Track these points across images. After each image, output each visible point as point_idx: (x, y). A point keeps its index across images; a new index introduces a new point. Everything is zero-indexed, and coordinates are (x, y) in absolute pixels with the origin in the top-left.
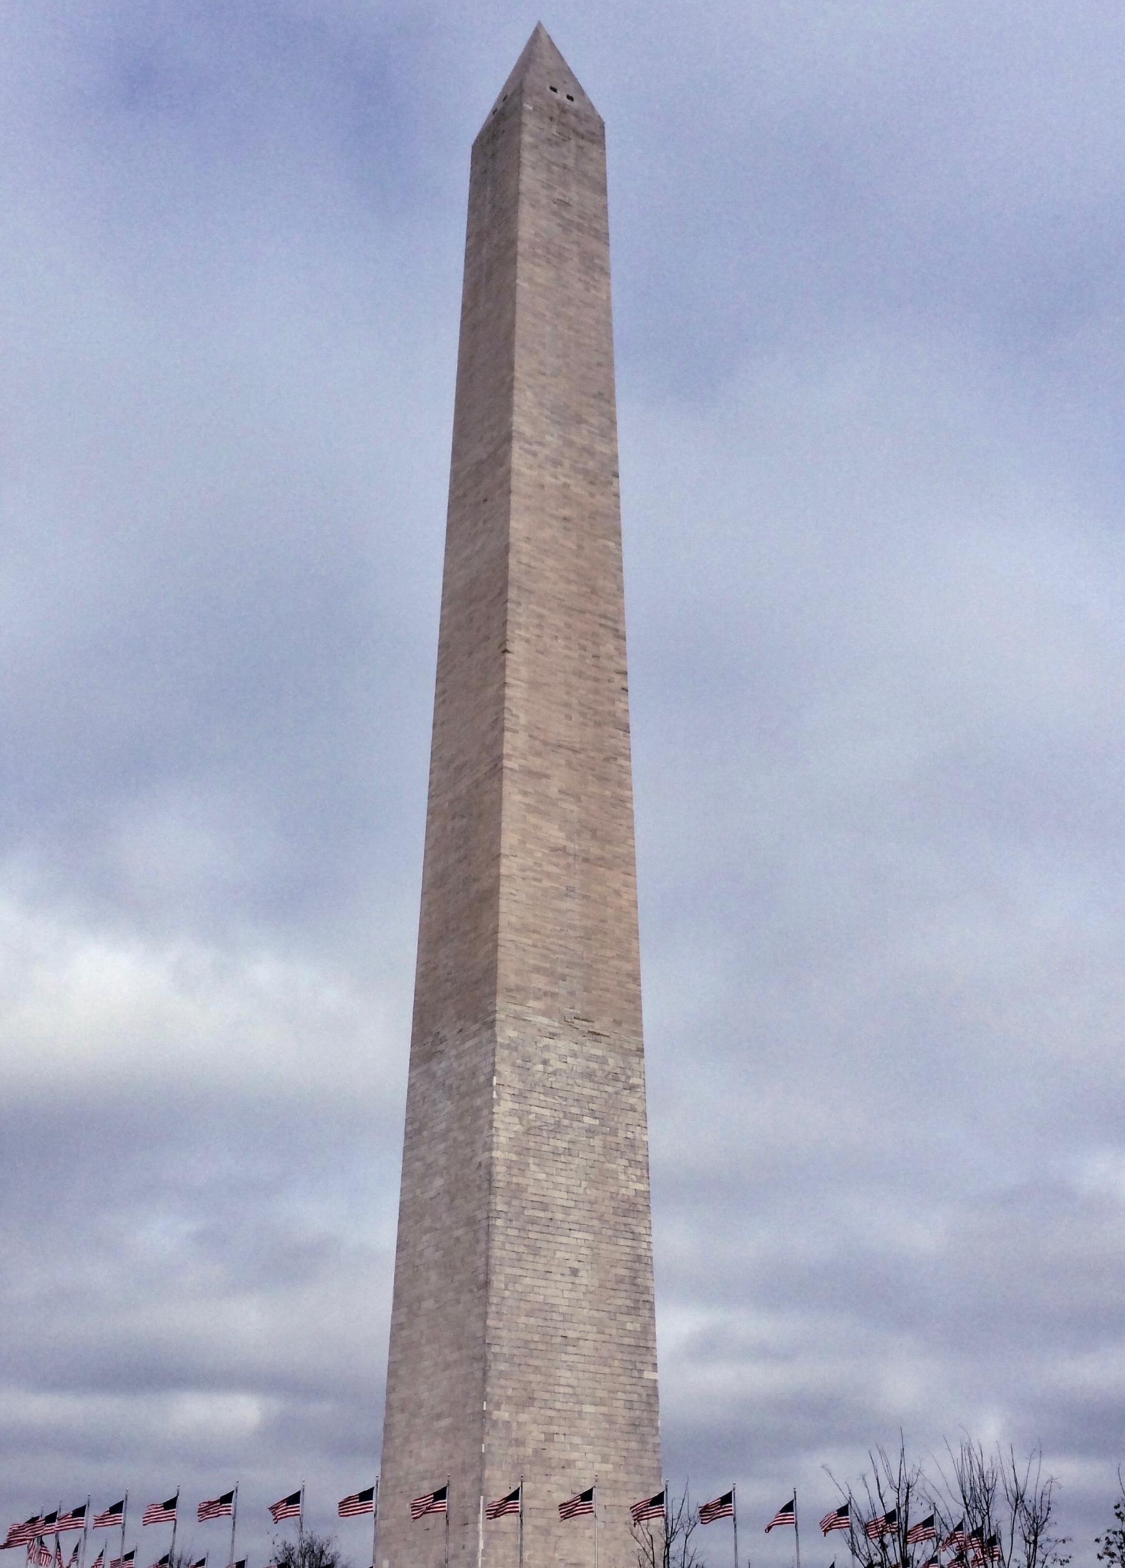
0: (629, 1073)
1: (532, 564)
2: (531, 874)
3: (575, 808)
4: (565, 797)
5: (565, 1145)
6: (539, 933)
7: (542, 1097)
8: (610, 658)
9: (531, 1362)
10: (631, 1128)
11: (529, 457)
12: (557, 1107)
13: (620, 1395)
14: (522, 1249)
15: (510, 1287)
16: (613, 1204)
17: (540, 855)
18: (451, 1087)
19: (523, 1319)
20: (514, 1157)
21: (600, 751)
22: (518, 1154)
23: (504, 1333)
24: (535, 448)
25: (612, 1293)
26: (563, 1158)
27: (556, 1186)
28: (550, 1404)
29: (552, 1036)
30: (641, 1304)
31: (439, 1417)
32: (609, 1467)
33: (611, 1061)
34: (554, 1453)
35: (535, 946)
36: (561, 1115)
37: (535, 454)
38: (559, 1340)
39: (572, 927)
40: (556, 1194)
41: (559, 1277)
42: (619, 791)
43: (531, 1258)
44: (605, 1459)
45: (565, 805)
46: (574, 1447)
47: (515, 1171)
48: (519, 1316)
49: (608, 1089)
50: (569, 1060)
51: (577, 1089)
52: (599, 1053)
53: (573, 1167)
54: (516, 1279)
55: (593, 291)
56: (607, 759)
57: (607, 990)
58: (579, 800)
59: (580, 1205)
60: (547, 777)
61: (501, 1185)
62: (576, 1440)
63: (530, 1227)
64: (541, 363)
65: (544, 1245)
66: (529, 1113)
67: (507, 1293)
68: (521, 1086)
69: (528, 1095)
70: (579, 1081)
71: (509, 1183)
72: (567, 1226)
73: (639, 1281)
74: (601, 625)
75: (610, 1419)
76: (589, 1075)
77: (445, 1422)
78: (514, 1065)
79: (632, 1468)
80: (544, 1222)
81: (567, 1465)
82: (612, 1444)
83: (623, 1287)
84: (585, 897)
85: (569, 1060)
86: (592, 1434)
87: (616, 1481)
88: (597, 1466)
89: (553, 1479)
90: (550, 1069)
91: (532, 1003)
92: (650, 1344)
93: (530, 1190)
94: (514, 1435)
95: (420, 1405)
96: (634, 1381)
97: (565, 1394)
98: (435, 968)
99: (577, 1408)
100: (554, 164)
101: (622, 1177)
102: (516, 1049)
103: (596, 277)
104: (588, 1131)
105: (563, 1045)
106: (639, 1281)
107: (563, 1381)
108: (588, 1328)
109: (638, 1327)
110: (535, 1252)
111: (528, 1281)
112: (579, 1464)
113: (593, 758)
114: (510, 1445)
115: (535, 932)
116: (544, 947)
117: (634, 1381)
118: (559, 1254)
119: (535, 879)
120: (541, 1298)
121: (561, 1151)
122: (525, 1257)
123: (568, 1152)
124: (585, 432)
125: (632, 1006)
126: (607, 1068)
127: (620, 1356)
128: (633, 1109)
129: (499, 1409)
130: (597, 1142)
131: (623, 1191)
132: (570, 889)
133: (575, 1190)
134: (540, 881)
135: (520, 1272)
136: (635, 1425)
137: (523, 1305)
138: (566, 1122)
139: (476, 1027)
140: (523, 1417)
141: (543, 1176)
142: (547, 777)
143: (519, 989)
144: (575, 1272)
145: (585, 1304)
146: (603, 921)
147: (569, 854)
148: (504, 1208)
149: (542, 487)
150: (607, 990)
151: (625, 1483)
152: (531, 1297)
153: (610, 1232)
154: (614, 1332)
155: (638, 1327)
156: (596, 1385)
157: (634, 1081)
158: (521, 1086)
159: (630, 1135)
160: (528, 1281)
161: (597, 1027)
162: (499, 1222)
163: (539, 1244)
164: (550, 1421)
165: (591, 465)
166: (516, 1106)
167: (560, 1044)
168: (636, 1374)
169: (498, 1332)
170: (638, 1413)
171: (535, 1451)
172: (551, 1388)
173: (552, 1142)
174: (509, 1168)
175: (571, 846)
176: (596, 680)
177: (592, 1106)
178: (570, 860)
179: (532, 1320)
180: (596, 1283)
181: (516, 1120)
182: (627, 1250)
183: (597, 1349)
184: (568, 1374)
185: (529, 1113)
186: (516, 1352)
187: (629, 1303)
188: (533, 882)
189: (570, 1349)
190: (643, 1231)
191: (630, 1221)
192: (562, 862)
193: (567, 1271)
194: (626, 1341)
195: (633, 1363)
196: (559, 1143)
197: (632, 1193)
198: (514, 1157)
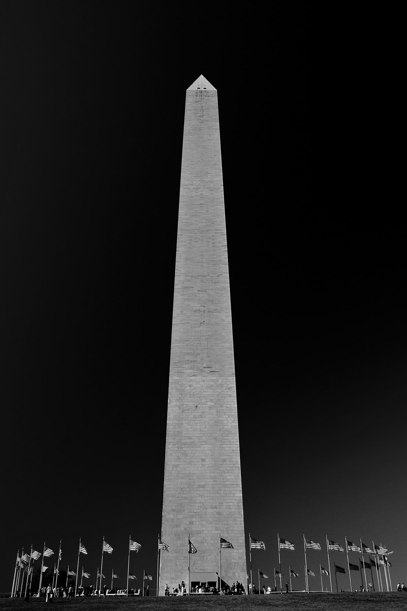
0: (228, 383)
7: (189, 398)
8: (220, 242)
9: (184, 496)
10: (229, 403)
14: (180, 454)
16: (221, 432)
17: (189, 314)
20: (177, 422)
22: (178, 420)
24: (189, 186)
25: (221, 466)
26: (198, 419)
33: (220, 380)
34: (194, 528)
43: (183, 457)
44: (217, 529)
49: (218, 390)
51: (204, 393)
52: (215, 378)
61: (171, 432)
62: (204, 523)
63: (183, 446)
67: (173, 472)
76: (210, 387)
86: (211, 520)
88: (213, 532)
90: (192, 388)
91: (184, 366)
99: (204, 511)
101: (226, 422)
105: (198, 378)
107: (197, 501)
111: (182, 466)
114: (174, 527)
118: (196, 454)
120: (188, 472)
129: (169, 514)
130: (214, 411)
134: (189, 323)
135: (177, 463)
137: (180, 475)
140: (180, 516)
143: (179, 362)
144: (203, 460)
152: (184, 472)
153: (220, 443)
154: (222, 480)
155: (233, 477)
159: (228, 406)
161: (213, 369)
162: (169, 446)
164: (192, 517)
165: (212, 185)
167: (198, 378)
170: (233, 510)
173: (193, 414)
175: (202, 309)
176: (215, 251)
177: (211, 398)
181: (178, 408)
183: (213, 488)
184: (200, 498)
185: (183, 405)
189: (201, 489)
193: (200, 460)
196: (196, 414)
198: (177, 422)
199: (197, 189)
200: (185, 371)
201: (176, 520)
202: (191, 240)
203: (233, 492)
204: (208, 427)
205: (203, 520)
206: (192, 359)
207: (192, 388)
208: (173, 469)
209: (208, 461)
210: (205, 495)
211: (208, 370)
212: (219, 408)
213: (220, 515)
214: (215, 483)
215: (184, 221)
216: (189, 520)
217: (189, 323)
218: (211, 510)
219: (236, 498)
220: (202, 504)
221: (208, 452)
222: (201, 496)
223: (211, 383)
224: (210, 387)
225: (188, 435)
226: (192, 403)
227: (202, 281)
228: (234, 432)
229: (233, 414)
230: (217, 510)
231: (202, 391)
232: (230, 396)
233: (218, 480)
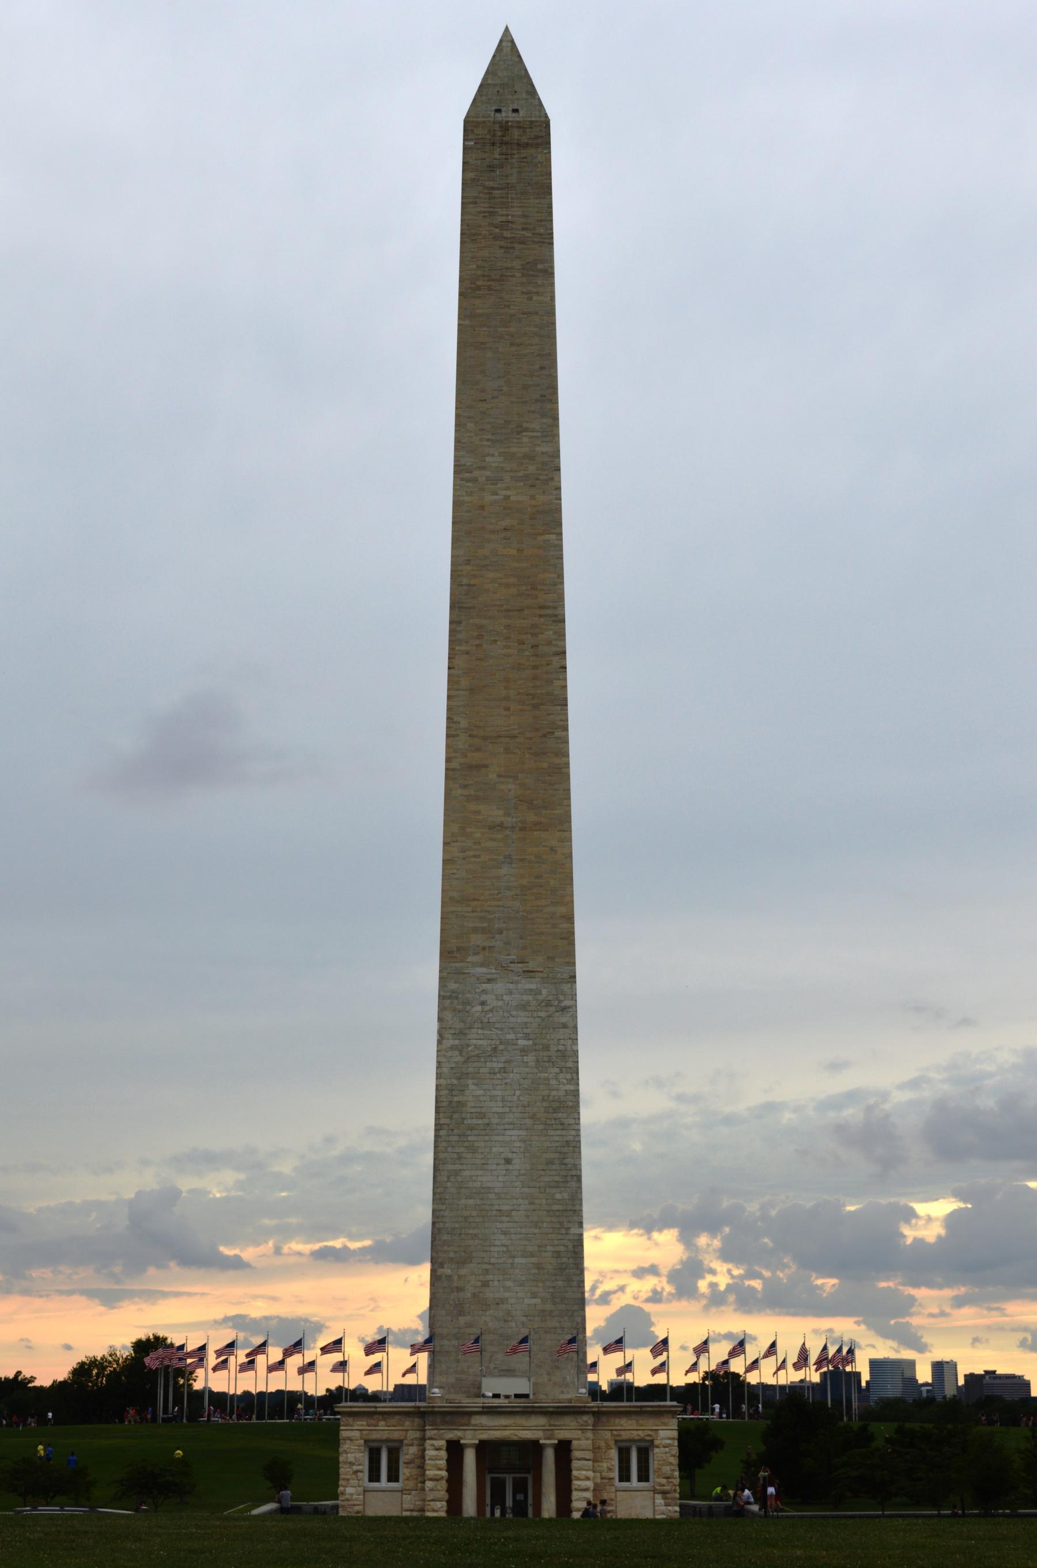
0: (562, 997)
1: (473, 582)
2: (471, 853)
3: (511, 786)
5: (501, 1065)
7: (480, 1031)
8: (549, 643)
9: (471, 1231)
11: (470, 484)
12: (494, 1037)
13: (549, 1248)
14: (462, 1150)
15: (452, 1179)
16: (545, 1104)
17: (478, 835)
20: (455, 1082)
21: (537, 730)
22: (459, 1079)
23: (446, 1214)
25: (542, 1173)
26: (498, 1076)
27: (493, 1098)
28: (486, 1260)
29: (489, 981)
32: (538, 1301)
33: (544, 992)
34: (490, 1294)
35: (473, 911)
36: (498, 1042)
37: (475, 480)
39: (509, 888)
40: (493, 1104)
41: (494, 1167)
42: (557, 761)
43: (469, 1155)
44: (534, 1295)
45: (503, 787)
46: (507, 1289)
47: (455, 1093)
48: (459, 1199)
50: (505, 997)
51: (512, 1019)
52: (533, 986)
54: (457, 1173)
55: (535, 298)
56: (545, 736)
57: (542, 933)
58: (516, 778)
60: (486, 766)
61: (444, 1104)
62: (509, 1284)
63: (469, 1132)
64: (483, 391)
65: (483, 1144)
68: (462, 1025)
69: (467, 1031)
70: (514, 1013)
71: (450, 1102)
73: (567, 1161)
74: (540, 616)
76: (523, 1007)
78: (455, 1010)
79: (557, 1300)
80: (482, 1127)
82: (540, 1284)
83: (554, 1167)
84: (522, 860)
85: (505, 997)
86: (523, 1278)
87: (543, 1311)
88: (526, 1301)
90: (487, 1008)
91: (470, 959)
92: (577, 1208)
93: (469, 1104)
94: (455, 1285)
96: (560, 1237)
97: (498, 1252)
99: (510, 1261)
100: (493, 189)
101: (553, 1082)
102: (457, 998)
103: (539, 282)
105: (500, 987)
106: (567, 1161)
107: (497, 1243)
108: (521, 1201)
109: (566, 1196)
110: (473, 1150)
111: (467, 1173)
113: (531, 739)
114: (452, 1291)
115: (474, 899)
117: (560, 1237)
118: (494, 1150)
119: (475, 856)
120: (478, 1184)
121: (497, 1070)
122: (464, 1155)
124: (525, 440)
125: (566, 942)
126: (540, 997)
127: (549, 1219)
128: (565, 1026)
130: (530, 1059)
131: (554, 1093)
135: (458, 1167)
136: (561, 1269)
138: (501, 1047)
140: (463, 1272)
142: (486, 766)
144: (508, 1161)
145: (518, 1184)
146: (539, 877)
147: (507, 828)
148: (448, 1121)
149: (482, 507)
150: (542, 933)
151: (551, 1311)
152: (471, 1184)
153: (541, 1127)
154: (544, 1201)
155: (566, 1196)
156: (527, 1243)
157: (567, 1003)
158: (462, 1025)
159: (561, 1048)
160: (467, 1173)
161: (531, 966)
163: (476, 1144)
164: (487, 1272)
165: (532, 469)
166: (457, 1042)
168: (563, 1231)
169: (442, 1213)
170: (564, 1260)
171: (474, 1295)
172: (488, 1248)
173: (489, 1064)
174: (451, 1090)
175: (508, 821)
176: (535, 667)
177: (525, 1031)
178: (507, 832)
179: (471, 1202)
180: (528, 1167)
181: (457, 1053)
183: (528, 1216)
184: (503, 1237)
185: (468, 1046)
186: (457, 1226)
187: (557, 1178)
188: (473, 859)
189: (504, 1219)
190: (572, 1121)
192: (500, 836)
193: (503, 1162)
194: (556, 1207)
196: (495, 1065)
198: (455, 1082)
199: (494, 481)
200: (472, 971)
201: (455, 1278)
202: (480, 637)
203: (566, 1225)
204: (518, 1093)
205: (508, 1280)
206: (487, 944)
207: (487, 1008)
208: (448, 1177)
209: (518, 1164)
210: (512, 1230)
211: (519, 967)
212: (541, 1053)
213: (539, 1268)
214: (533, 1207)
215: (465, 581)
216: (482, 1278)
219: (571, 1237)
220: (505, 1249)
221: (517, 1144)
222: (505, 1234)
223: (525, 998)
224: (523, 1007)
225: (478, 1110)
226: (484, 1043)
227: (507, 751)
230: (534, 1260)
231: (506, 1014)
233: (537, 1201)
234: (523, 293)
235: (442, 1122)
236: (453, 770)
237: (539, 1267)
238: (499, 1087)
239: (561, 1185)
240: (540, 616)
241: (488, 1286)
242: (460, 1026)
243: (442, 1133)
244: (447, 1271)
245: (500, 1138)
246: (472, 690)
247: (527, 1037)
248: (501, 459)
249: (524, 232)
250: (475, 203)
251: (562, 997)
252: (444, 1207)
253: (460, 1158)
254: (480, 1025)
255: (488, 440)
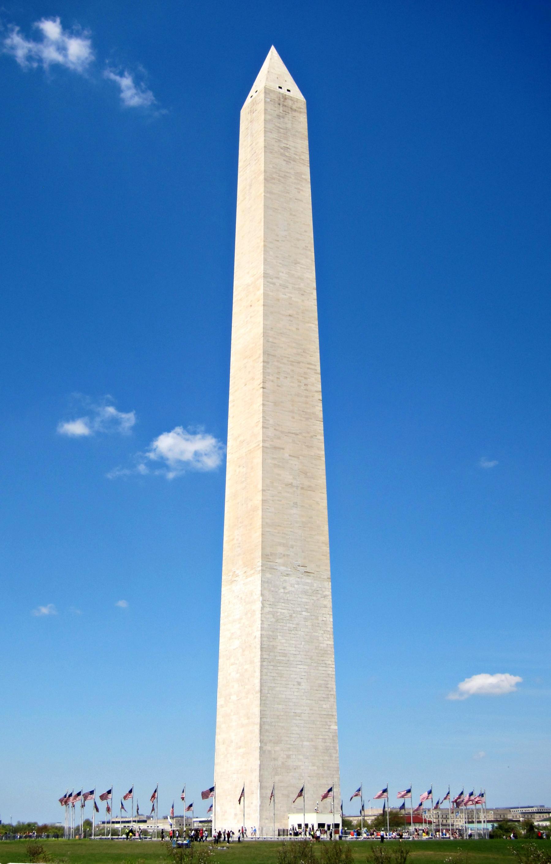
0: (324, 589)
4: (293, 458)
5: (294, 626)
6: (280, 526)
7: (283, 604)
8: (313, 385)
9: (280, 724)
11: (271, 285)
13: (321, 737)
14: (275, 675)
16: (317, 651)
18: (241, 598)
19: (276, 706)
20: (271, 633)
21: (308, 433)
22: (273, 632)
24: (275, 280)
25: (316, 692)
26: (293, 632)
29: (288, 575)
30: (330, 696)
31: (240, 747)
32: (316, 768)
33: (315, 585)
35: (278, 533)
36: (292, 612)
38: (292, 714)
40: (290, 649)
41: (292, 686)
43: (279, 678)
51: (299, 600)
52: (309, 581)
53: (298, 635)
56: (312, 437)
58: (298, 458)
59: (301, 653)
60: (283, 449)
63: (278, 665)
66: (277, 612)
69: (276, 604)
72: (295, 663)
73: (329, 686)
74: (308, 368)
75: (316, 748)
76: (305, 592)
77: (242, 750)
81: (296, 768)
84: (302, 506)
85: (296, 586)
87: (319, 774)
88: (310, 768)
89: (290, 774)
90: (286, 591)
93: (279, 648)
95: (232, 742)
96: (326, 730)
98: (233, 539)
103: (303, 185)
104: (305, 618)
105: (292, 579)
107: (294, 732)
108: (306, 708)
111: (278, 689)
112: (302, 767)
113: (305, 437)
115: (278, 526)
116: (283, 533)
117: (326, 730)
119: (278, 500)
120: (284, 696)
123: (296, 629)
124: (298, 268)
129: (266, 745)
130: (308, 623)
132: (296, 503)
133: (299, 646)
134: (280, 501)
135: (274, 685)
139: (252, 572)
140: (277, 748)
141: (284, 641)
142: (283, 449)
143: (272, 554)
144: (299, 684)
145: (304, 697)
147: (294, 486)
148: (267, 657)
152: (280, 696)
153: (315, 665)
159: (324, 619)
160: (278, 689)
164: (289, 749)
165: (302, 285)
166: (271, 610)
168: (327, 727)
170: (328, 744)
171: (283, 763)
173: (288, 625)
176: (307, 397)
177: (306, 607)
179: (280, 706)
181: (271, 616)
182: (323, 672)
183: (309, 717)
184: (297, 729)
187: (324, 696)
189: (297, 718)
191: (324, 658)
193: (296, 683)
195: (326, 722)
197: (325, 645)
198: (271, 633)
211: (302, 569)
217: (280, 501)
218: (308, 743)
220: (298, 736)
221: (303, 674)
224: (305, 592)
226: (285, 611)
228: (329, 652)
229: (329, 629)
232: (325, 607)
234: (295, 188)
235: (265, 657)
236: (266, 447)
237: (316, 748)
238: (294, 639)
239: (326, 699)
240: (308, 368)
241: (290, 758)
242: (272, 600)
243: (265, 663)
244: (268, 747)
245: (295, 669)
246: (275, 404)
247: (307, 610)
248: (287, 276)
249: (295, 156)
250: (271, 132)
251: (324, 589)
252: (266, 709)
253: (274, 680)
254: (282, 601)
255: (280, 263)
